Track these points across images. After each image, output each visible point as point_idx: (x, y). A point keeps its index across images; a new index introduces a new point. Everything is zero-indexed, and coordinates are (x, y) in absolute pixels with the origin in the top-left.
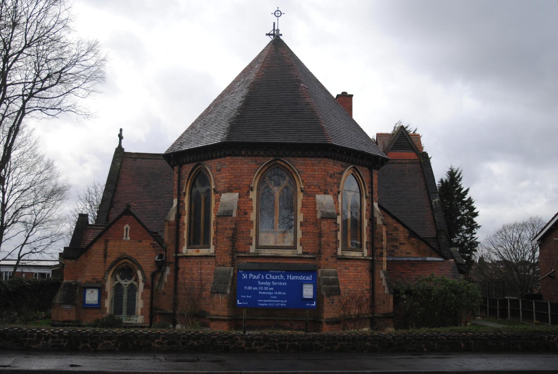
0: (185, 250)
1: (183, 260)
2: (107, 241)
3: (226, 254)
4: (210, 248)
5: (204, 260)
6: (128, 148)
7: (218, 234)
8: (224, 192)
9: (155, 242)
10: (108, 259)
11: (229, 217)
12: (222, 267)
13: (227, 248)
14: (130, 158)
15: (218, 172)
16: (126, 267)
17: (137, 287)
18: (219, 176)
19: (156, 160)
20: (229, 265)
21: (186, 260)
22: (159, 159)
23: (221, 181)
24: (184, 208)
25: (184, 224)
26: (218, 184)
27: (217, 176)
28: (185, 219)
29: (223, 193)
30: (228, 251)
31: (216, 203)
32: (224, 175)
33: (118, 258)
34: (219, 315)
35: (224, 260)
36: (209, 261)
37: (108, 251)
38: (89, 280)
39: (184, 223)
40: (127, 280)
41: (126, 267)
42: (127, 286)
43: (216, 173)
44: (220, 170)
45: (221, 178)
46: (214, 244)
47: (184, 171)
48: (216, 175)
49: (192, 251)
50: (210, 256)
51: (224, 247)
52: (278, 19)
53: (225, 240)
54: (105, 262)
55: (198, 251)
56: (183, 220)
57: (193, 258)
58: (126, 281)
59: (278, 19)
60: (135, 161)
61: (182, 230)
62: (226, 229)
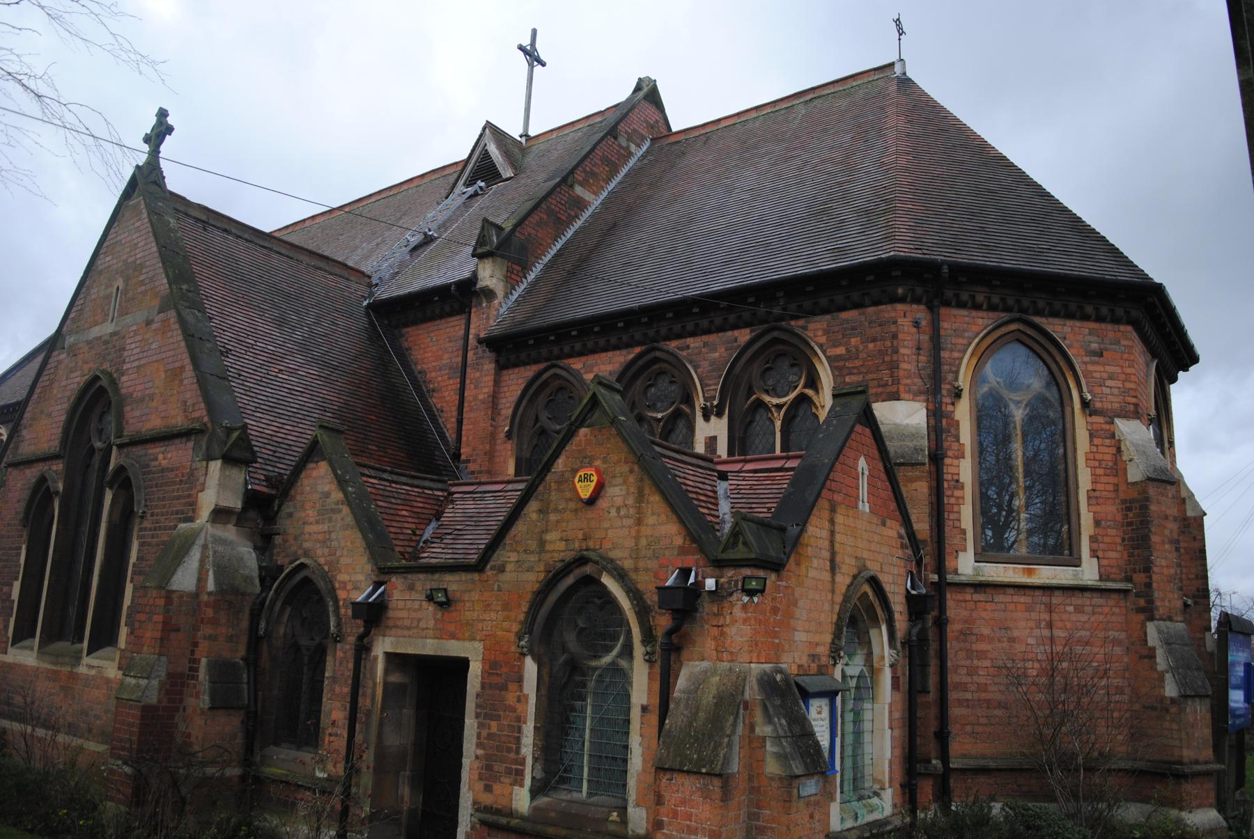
0: (966, 565)
1: (959, 597)
2: (833, 510)
3: (1172, 585)
4: (1078, 566)
5: (1057, 599)
6: (177, 181)
7: (1153, 529)
8: (1125, 415)
10: (839, 578)
11: (1169, 487)
12: (1168, 623)
13: (1172, 571)
14: (186, 214)
15: (1096, 359)
18: (1101, 368)
19: (265, 251)
20: (1180, 619)
21: (977, 597)
22: (271, 249)
23: (1108, 383)
25: (958, 485)
26: (1097, 390)
27: (1090, 368)
28: (965, 470)
29: (1119, 416)
30: (1175, 579)
31: (1091, 441)
32: (1118, 370)
34: (1201, 759)
35: (1169, 601)
36: (1079, 602)
37: (837, 546)
38: (804, 660)
39: (957, 481)
43: (1087, 359)
44: (1101, 355)
45: (1105, 375)
46: (1094, 553)
48: (1086, 363)
49: (1002, 570)
50: (1082, 589)
51: (1167, 566)
52: (900, 39)
53: (1167, 546)
54: (833, 591)
55: (1030, 572)
56: (951, 470)
57: (1011, 591)
59: (900, 39)
60: (205, 230)
61: (952, 500)
62: (1166, 517)
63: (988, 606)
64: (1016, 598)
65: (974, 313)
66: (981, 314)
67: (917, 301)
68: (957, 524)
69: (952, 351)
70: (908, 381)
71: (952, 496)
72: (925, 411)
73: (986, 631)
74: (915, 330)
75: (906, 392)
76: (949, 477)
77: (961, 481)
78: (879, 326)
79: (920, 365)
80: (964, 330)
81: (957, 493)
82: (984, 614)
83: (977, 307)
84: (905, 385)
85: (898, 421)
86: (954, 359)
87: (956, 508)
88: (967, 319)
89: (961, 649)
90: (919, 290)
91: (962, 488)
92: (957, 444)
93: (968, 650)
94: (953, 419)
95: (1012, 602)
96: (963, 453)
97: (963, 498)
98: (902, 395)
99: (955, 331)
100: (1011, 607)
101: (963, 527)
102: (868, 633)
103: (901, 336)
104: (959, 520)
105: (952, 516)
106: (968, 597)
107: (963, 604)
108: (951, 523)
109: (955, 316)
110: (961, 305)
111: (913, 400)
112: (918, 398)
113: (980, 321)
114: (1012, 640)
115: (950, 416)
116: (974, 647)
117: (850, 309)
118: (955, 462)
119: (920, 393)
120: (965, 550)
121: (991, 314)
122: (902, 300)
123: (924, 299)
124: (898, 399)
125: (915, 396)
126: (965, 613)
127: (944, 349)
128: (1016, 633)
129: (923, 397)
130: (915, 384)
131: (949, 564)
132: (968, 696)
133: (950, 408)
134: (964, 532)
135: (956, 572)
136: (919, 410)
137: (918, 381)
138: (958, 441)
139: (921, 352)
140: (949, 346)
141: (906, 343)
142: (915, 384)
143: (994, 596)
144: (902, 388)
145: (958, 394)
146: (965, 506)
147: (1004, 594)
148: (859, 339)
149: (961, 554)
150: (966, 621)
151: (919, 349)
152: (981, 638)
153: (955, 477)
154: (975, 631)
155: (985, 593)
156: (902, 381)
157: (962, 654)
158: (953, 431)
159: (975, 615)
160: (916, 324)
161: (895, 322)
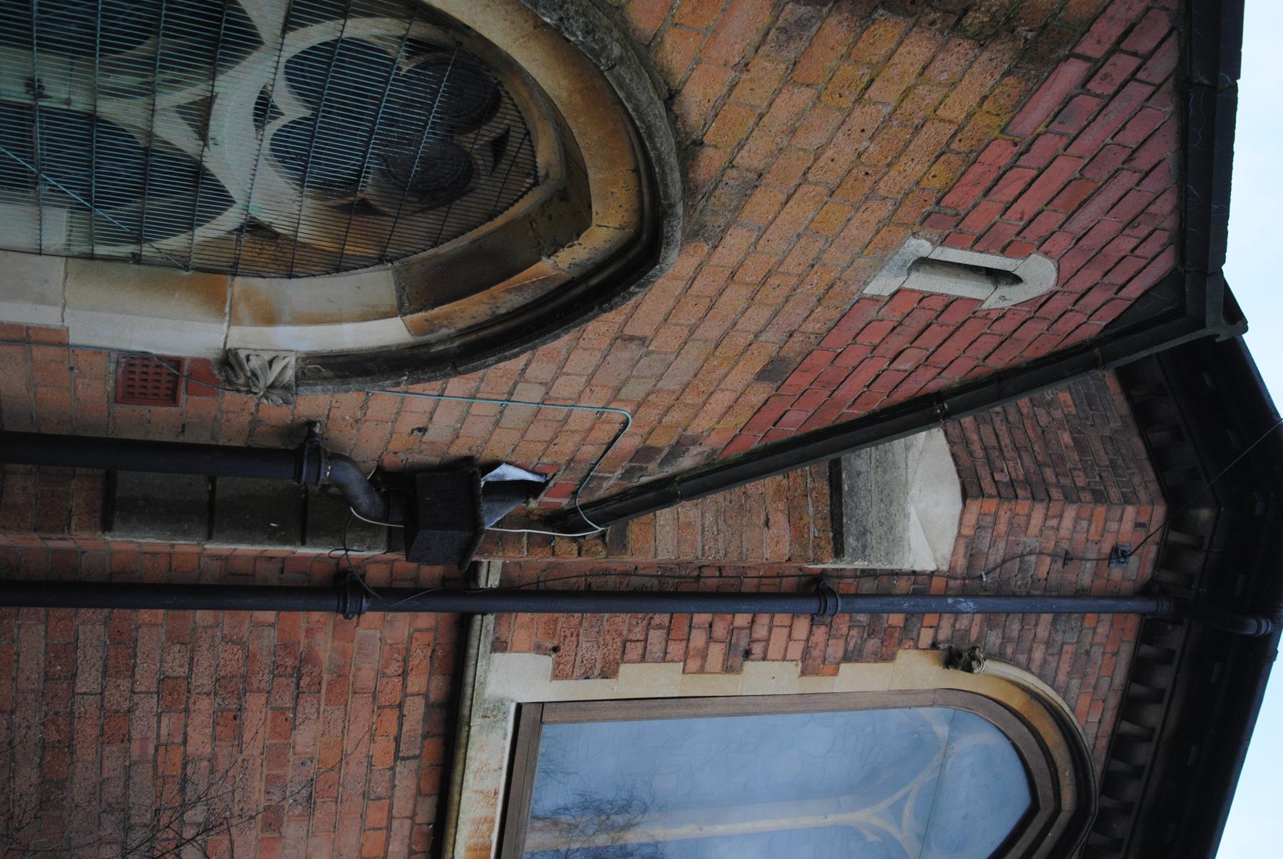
1: (420, 656)
9: (687, 462)
16: (498, 146)
17: (147, 250)
21: (415, 710)
24: (851, 656)
33: (689, 149)
39: (747, 654)
40: (273, 127)
41: (498, 146)
42: (177, 134)
47: (1102, 629)
56: (779, 636)
57: (426, 812)
58: (264, 108)
61: (698, 638)
63: (384, 746)
64: (401, 828)
65: (1113, 701)
66: (1109, 717)
67: (1168, 556)
68: (634, 651)
69: (1048, 644)
70: (1002, 527)
71: (710, 638)
72: (930, 566)
73: (304, 738)
74: (1107, 548)
75: (981, 514)
76: (760, 632)
77: (749, 666)
78: (1111, 461)
79: (1033, 558)
80: (1084, 676)
81: (716, 652)
82: (358, 730)
83: (1128, 707)
84: (996, 517)
85: (914, 491)
86: (1030, 651)
87: (676, 648)
88: (1105, 683)
89: (249, 657)
90: (1195, 563)
91: (728, 669)
92: (840, 654)
93: (245, 678)
94: (900, 644)
95: (391, 818)
96: (816, 673)
97: (702, 670)
98: (974, 507)
99: (1088, 653)
100: (377, 816)
101: (624, 668)
102: (381, 260)
103: (1101, 510)
104: (643, 659)
105: (656, 637)
106: (417, 683)
107: (394, 668)
108: (638, 633)
109: (1115, 654)
110: (1139, 670)
111: (959, 535)
112: (961, 551)
113: (1094, 718)
114: (273, 820)
115: (906, 636)
116: (255, 703)
117: (1129, 398)
118: (796, 650)
119: (972, 557)
120: (556, 676)
121: (1103, 742)
122: (1175, 520)
123: (1166, 576)
124: (965, 495)
125: (969, 545)
126: (366, 673)
127: (1054, 623)
128: (292, 831)
129: (961, 563)
130: (993, 543)
131: (525, 624)
132: (88, 681)
133: (926, 637)
134: (608, 672)
135: (500, 646)
136: (934, 550)
137: (997, 555)
138: (847, 658)
139: (1059, 565)
140: (1059, 638)
141: (1085, 524)
142: (993, 543)
143: (412, 764)
144: (990, 505)
145: (957, 658)
146: (679, 677)
147: (419, 792)
148: (1073, 410)
149: (547, 662)
150: (341, 674)
151: (1067, 558)
152: (285, 722)
153: (757, 649)
154: (307, 706)
155: (425, 736)
156: (1006, 505)
157: (231, 659)
158: (873, 644)
159: (361, 708)
160: (1119, 554)
161: (1126, 500)
